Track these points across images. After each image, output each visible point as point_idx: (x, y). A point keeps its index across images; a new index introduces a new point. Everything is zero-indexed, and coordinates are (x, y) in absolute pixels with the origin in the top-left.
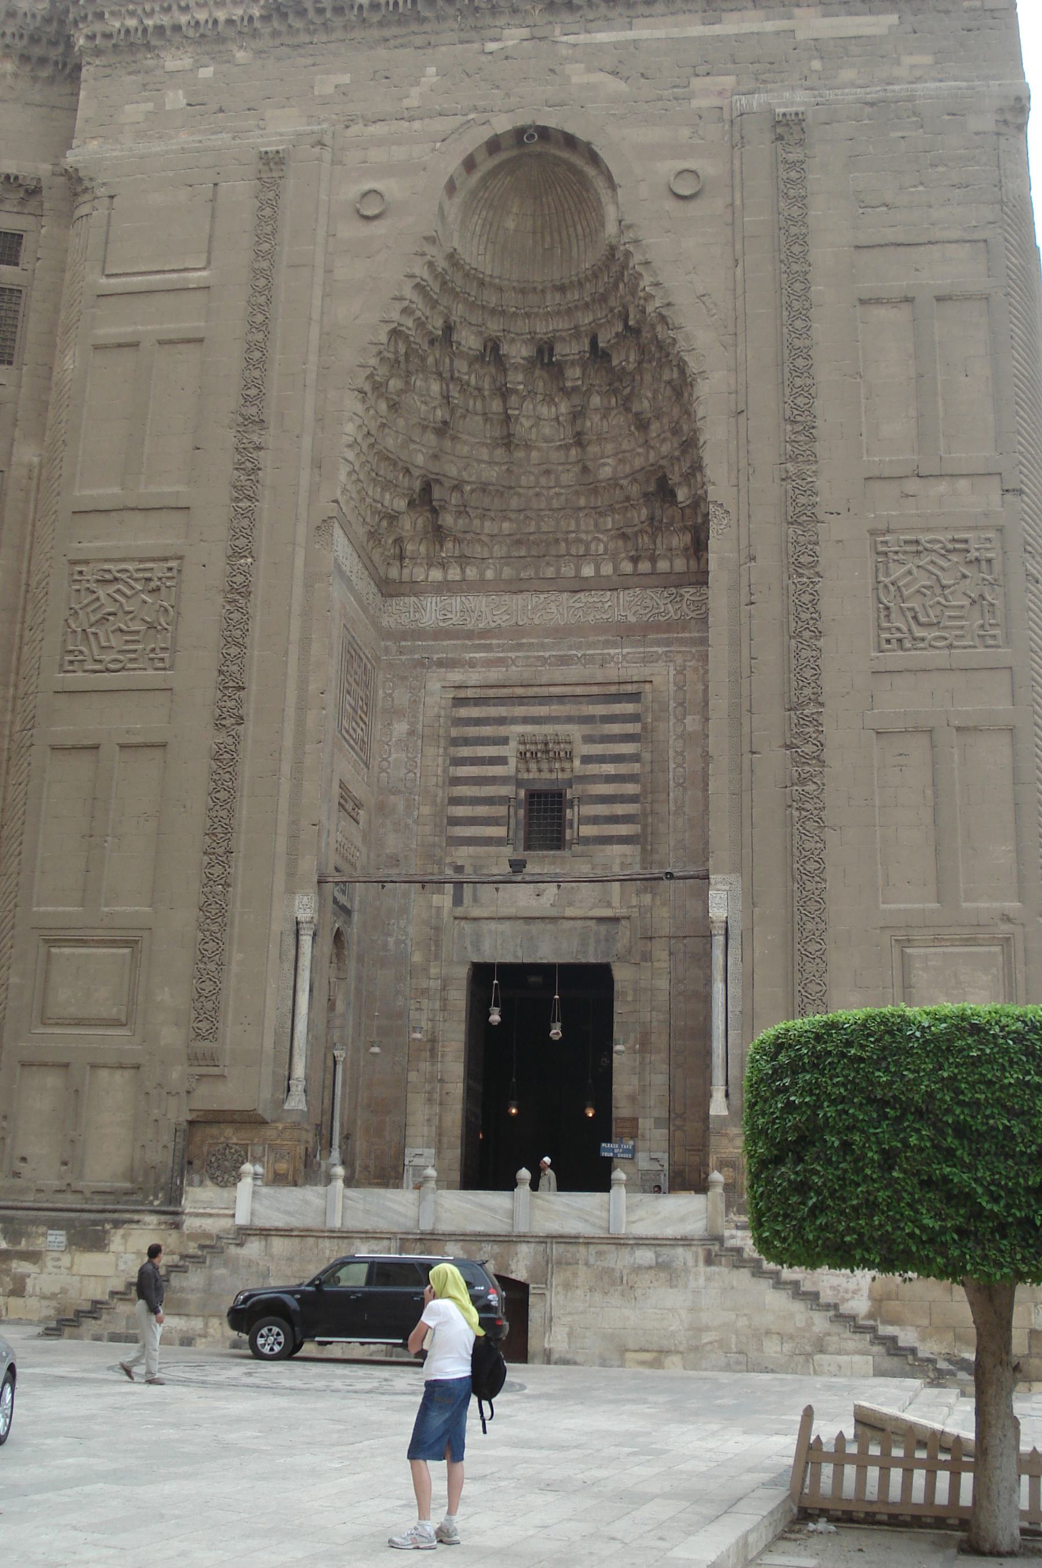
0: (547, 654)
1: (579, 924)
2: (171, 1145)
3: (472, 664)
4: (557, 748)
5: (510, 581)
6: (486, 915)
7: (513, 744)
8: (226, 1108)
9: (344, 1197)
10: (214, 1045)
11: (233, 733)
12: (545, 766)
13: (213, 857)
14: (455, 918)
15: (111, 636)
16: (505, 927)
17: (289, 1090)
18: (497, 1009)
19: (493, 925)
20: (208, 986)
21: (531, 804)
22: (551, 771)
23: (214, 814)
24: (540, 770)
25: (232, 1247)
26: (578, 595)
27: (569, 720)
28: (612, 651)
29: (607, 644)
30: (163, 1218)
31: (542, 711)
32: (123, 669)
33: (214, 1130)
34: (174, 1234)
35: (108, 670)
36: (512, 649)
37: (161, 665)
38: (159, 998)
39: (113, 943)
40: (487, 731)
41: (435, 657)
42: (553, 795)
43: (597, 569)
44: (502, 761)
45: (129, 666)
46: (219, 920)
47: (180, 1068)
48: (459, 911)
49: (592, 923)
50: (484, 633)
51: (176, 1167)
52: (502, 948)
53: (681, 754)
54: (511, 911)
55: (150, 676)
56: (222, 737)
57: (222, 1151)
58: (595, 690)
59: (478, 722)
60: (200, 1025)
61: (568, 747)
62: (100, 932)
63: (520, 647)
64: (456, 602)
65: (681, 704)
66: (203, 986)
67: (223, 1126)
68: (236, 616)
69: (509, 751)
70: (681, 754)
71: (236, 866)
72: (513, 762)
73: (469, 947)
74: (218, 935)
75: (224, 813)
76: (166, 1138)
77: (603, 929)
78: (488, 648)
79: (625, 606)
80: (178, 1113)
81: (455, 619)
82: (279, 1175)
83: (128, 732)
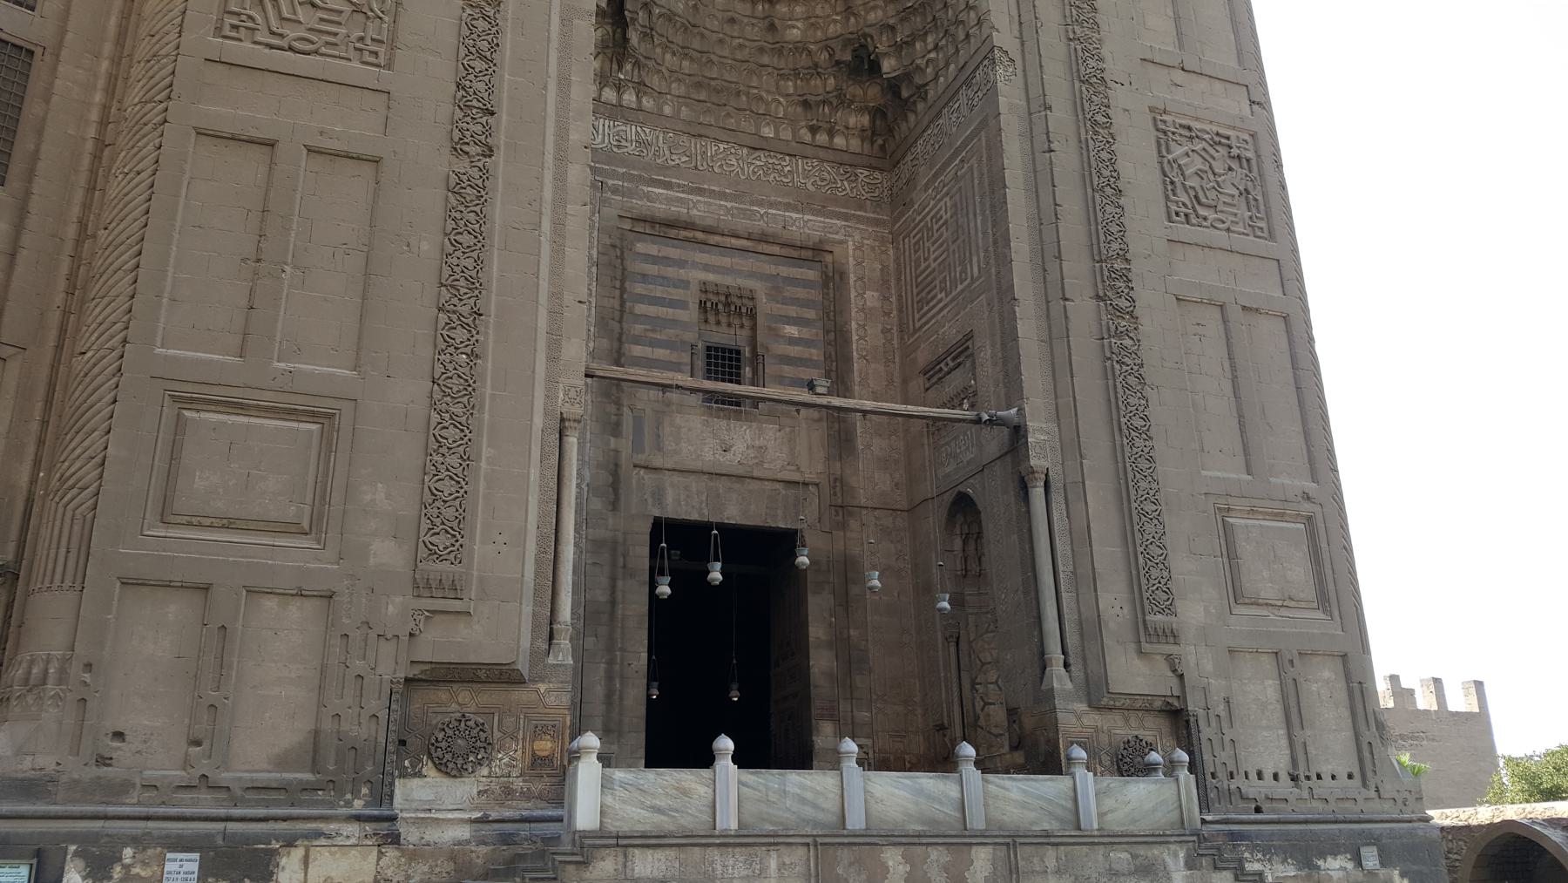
0: (729, 205)
1: (768, 486)
2: (383, 715)
3: (648, 196)
4: (738, 302)
5: (689, 123)
6: (669, 466)
7: (694, 288)
8: (472, 659)
9: (739, 782)
10: (457, 568)
11: (480, 164)
12: (724, 320)
13: (454, 317)
14: (635, 466)
15: (298, 8)
16: (694, 483)
17: (551, 637)
18: (718, 565)
19: (676, 478)
20: (447, 487)
21: (709, 357)
22: (729, 325)
23: (455, 261)
24: (718, 323)
25: (571, 868)
26: (757, 154)
27: (752, 275)
28: (795, 215)
29: (788, 207)
30: (368, 827)
31: (726, 261)
32: (316, 52)
33: (442, 694)
34: (391, 853)
35: (291, 49)
36: (692, 191)
37: (372, 59)
38: (368, 497)
39: (291, 413)
40: (671, 272)
41: (610, 182)
42: (731, 351)
43: (777, 132)
44: (683, 305)
45: (323, 50)
46: (465, 400)
47: (399, 599)
48: (640, 458)
49: (777, 486)
50: (664, 168)
51: (391, 748)
52: (685, 503)
53: (863, 326)
54: (698, 465)
55: (355, 70)
56: (462, 165)
57: (471, 723)
58: (776, 250)
59: (655, 260)
60: (434, 539)
61: (750, 304)
62: (269, 395)
63: (700, 191)
64: (632, 131)
65: (861, 279)
66: (439, 485)
67: (455, 686)
68: (481, 24)
69: (692, 297)
70: (863, 326)
71: (487, 334)
72: (694, 306)
73: (650, 501)
74: (463, 420)
75: (470, 263)
76: (376, 704)
77: (792, 491)
78: (668, 186)
79: (806, 174)
80: (389, 666)
81: (631, 148)
82: (541, 758)
83: (321, 133)
